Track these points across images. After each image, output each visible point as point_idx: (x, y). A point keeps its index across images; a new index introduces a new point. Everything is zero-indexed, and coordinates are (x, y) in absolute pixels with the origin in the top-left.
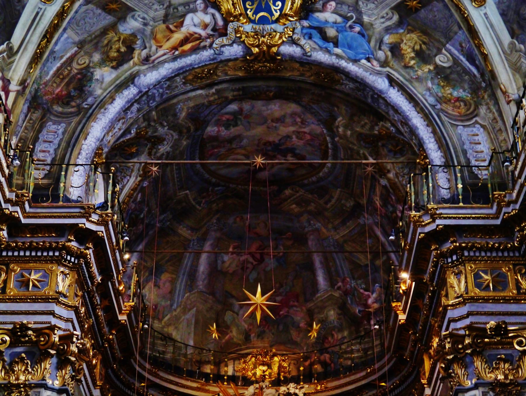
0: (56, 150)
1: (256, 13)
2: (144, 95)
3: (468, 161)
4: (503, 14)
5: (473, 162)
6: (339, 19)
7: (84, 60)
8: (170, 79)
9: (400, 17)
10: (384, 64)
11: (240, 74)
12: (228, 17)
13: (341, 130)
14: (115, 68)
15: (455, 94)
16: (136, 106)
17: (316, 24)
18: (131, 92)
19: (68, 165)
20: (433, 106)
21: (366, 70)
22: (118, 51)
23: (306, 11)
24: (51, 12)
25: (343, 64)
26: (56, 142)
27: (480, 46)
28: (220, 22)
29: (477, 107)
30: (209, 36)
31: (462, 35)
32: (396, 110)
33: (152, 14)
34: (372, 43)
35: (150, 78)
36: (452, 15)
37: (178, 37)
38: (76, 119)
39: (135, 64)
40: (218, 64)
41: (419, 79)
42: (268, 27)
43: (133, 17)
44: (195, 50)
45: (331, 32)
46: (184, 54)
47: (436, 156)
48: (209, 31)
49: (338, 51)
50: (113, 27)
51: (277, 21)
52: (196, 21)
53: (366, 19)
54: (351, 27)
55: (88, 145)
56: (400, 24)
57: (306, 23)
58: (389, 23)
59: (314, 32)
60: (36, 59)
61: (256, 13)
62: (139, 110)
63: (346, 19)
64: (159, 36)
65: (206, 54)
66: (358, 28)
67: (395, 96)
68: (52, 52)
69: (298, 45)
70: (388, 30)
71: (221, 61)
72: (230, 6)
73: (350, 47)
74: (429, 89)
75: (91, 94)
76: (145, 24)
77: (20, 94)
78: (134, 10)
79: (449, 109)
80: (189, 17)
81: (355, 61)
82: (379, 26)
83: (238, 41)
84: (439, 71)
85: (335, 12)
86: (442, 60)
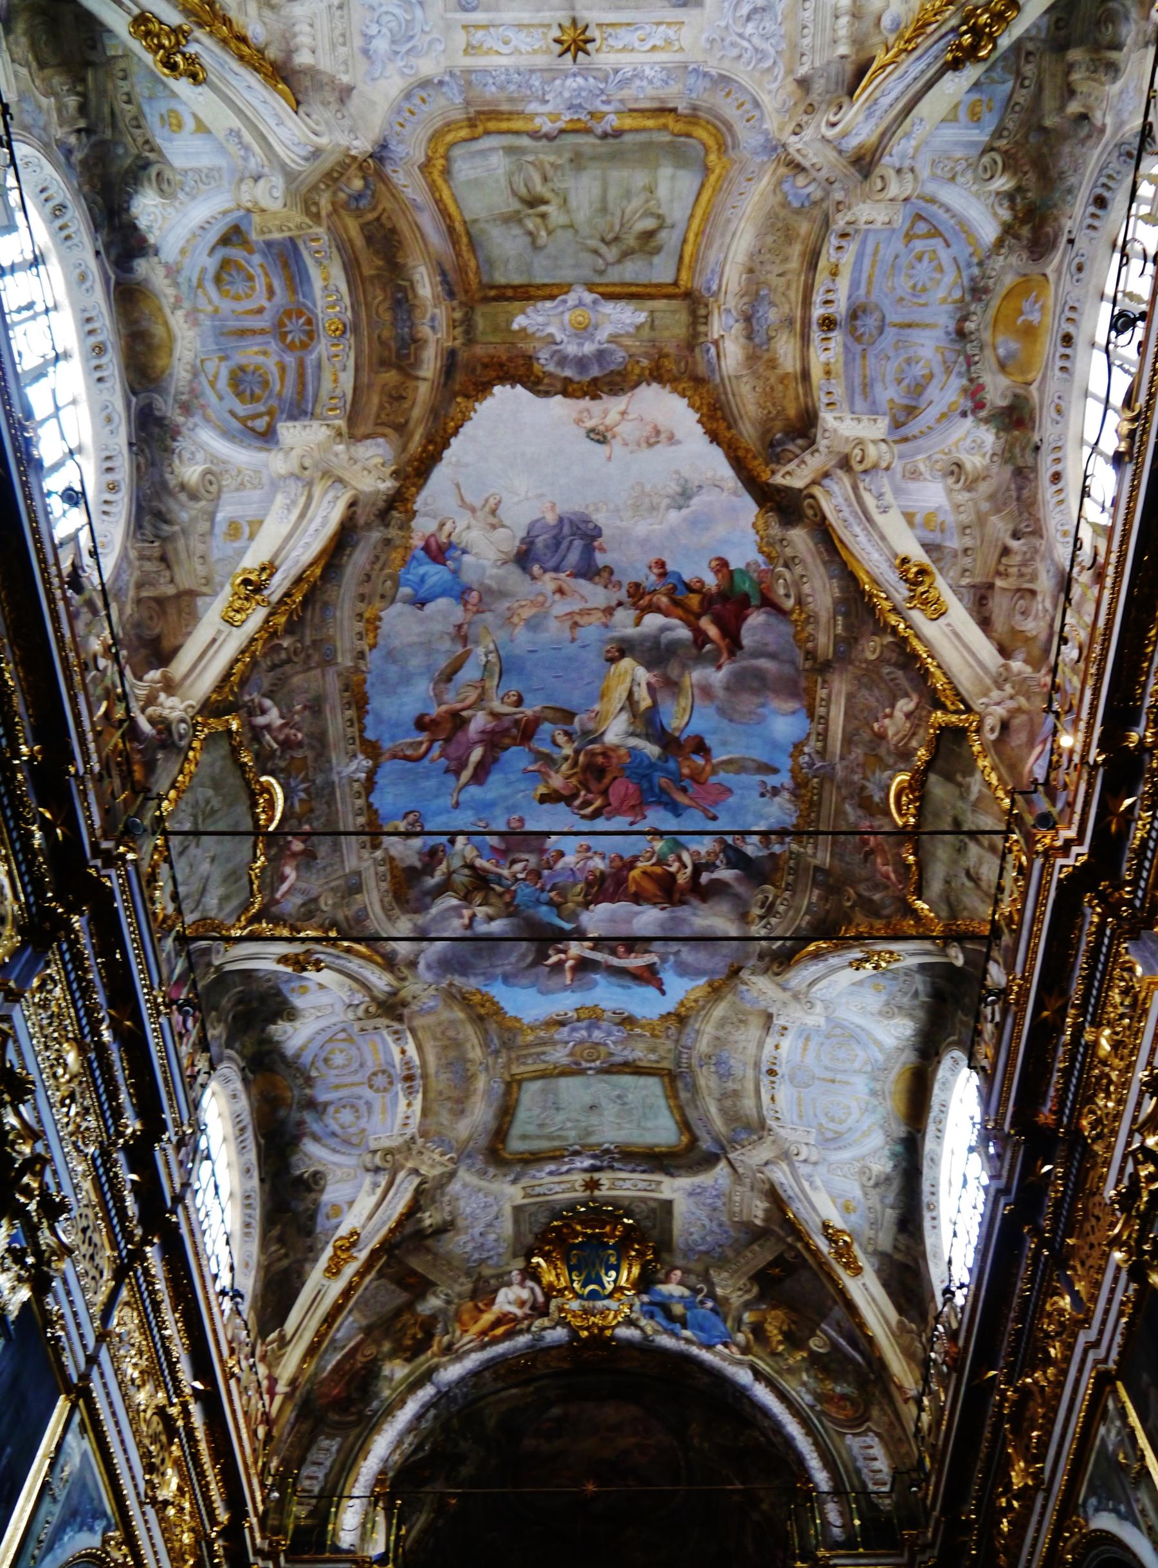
0: (327, 1476)
1: (584, 1286)
2: (443, 1397)
3: (864, 1485)
4: (886, 1285)
5: (871, 1487)
6: (687, 1292)
7: (371, 1350)
8: (475, 1374)
9: (761, 1289)
10: (745, 1350)
11: (566, 1366)
12: (550, 1292)
13: (696, 1441)
14: (408, 1360)
15: (838, 1389)
16: (432, 1412)
17: (658, 1299)
18: (427, 1392)
19: (341, 1497)
20: (812, 1407)
21: (724, 1358)
22: (414, 1337)
23: (644, 1284)
24: (336, 1287)
25: (695, 1350)
26: (328, 1463)
27: (862, 1325)
28: (541, 1299)
29: (867, 1409)
30: (527, 1317)
31: (838, 1312)
32: (765, 1412)
33: (458, 1288)
34: (729, 1324)
35: (452, 1372)
36: (823, 1286)
37: (487, 1318)
38: (356, 1431)
39: (434, 1355)
40: (538, 1352)
41: (791, 1371)
42: (600, 1304)
43: (435, 1294)
44: (509, 1335)
45: (678, 1309)
46: (495, 1341)
47: (821, 1478)
48: (527, 1310)
49: (687, 1333)
50: (410, 1306)
51: (610, 1296)
52: (512, 1297)
53: (719, 1291)
54: (702, 1303)
55: (369, 1467)
56: (760, 1298)
57: (645, 1298)
58: (747, 1297)
59: (656, 1310)
60: (312, 1350)
61: (584, 1286)
62: (436, 1417)
63: (696, 1291)
64: (466, 1317)
65: (523, 1340)
66: (710, 1304)
67: (762, 1393)
68: (333, 1341)
69: (637, 1327)
70: (747, 1306)
71: (543, 1350)
72: (552, 1278)
73: (702, 1328)
74: (804, 1384)
75: (377, 1395)
76: (448, 1302)
77: (288, 1397)
78: (433, 1284)
79: (833, 1411)
80: (503, 1291)
81: (709, 1347)
82: (736, 1299)
83: (563, 1322)
84: (814, 1360)
85: (681, 1283)
86: (815, 1344)
